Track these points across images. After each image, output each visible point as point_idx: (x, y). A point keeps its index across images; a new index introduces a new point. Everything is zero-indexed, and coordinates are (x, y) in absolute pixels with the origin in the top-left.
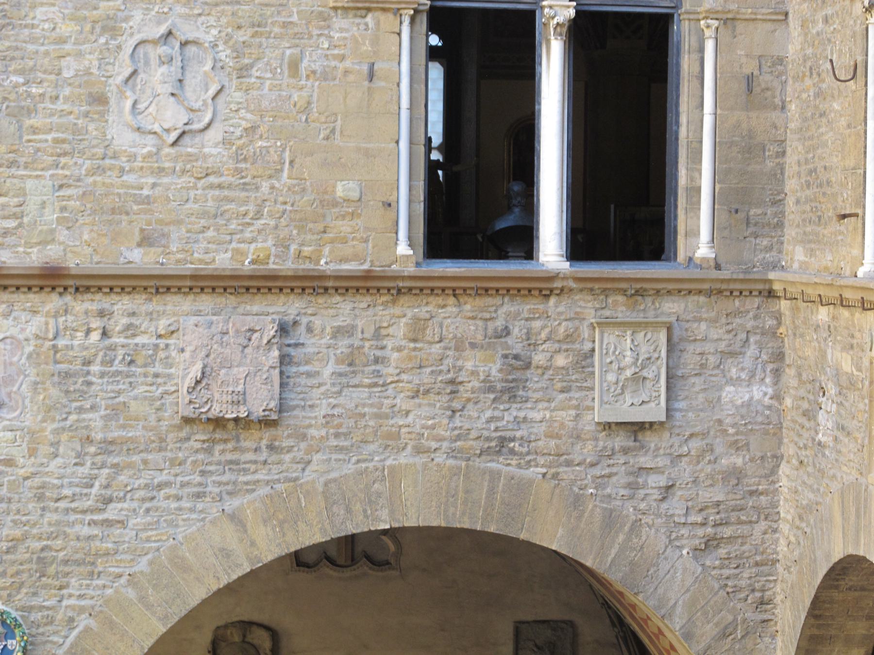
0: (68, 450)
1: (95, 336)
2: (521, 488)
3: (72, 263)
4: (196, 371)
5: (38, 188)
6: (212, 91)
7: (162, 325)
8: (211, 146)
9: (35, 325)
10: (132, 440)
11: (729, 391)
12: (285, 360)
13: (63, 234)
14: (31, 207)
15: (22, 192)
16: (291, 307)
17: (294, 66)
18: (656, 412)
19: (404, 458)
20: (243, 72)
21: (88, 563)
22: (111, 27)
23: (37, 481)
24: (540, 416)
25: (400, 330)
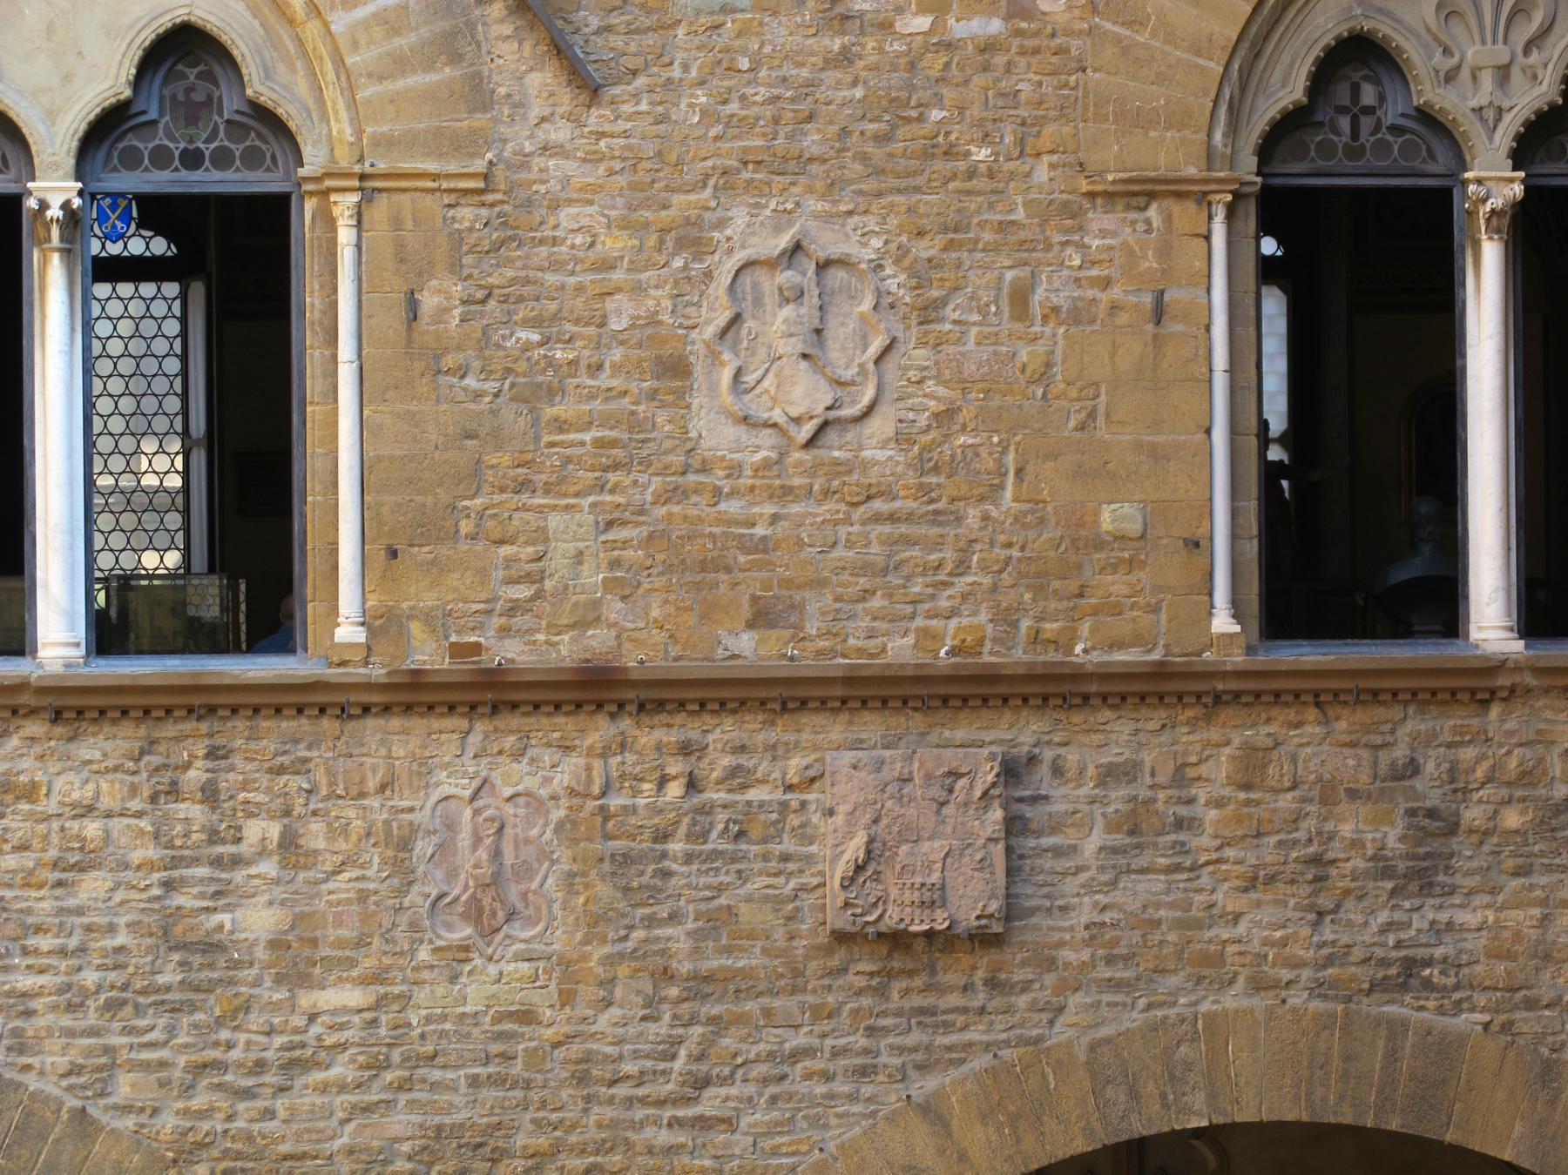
1: (675, 790)
2: (1445, 1050)
3: (631, 659)
4: (855, 848)
5: (569, 529)
6: (874, 349)
7: (794, 766)
8: (875, 445)
9: (567, 772)
10: (745, 973)
12: (1014, 826)
13: (614, 609)
14: (559, 561)
15: (541, 536)
16: (1025, 731)
17: (1020, 299)
19: (1233, 1000)
20: (928, 312)
22: (693, 239)
23: (576, 1049)
25: (1219, 769)
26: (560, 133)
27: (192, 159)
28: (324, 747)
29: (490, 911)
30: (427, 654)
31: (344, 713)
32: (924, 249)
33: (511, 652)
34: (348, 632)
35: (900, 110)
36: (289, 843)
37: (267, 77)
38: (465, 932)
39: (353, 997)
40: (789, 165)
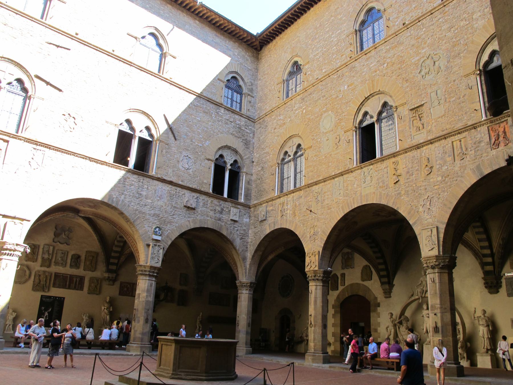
0: (170, 206)
2: (221, 226)
4: (187, 200)
5: (170, 171)
7: (183, 193)
11: (244, 219)
18: (237, 219)
19: (209, 218)
20: (195, 163)
21: (170, 223)
22: (181, 153)
24: (225, 217)
25: (210, 201)
29: (161, 197)
30: (159, 176)
31: (153, 179)
36: (147, 188)
39: (151, 201)
40: (188, 150)
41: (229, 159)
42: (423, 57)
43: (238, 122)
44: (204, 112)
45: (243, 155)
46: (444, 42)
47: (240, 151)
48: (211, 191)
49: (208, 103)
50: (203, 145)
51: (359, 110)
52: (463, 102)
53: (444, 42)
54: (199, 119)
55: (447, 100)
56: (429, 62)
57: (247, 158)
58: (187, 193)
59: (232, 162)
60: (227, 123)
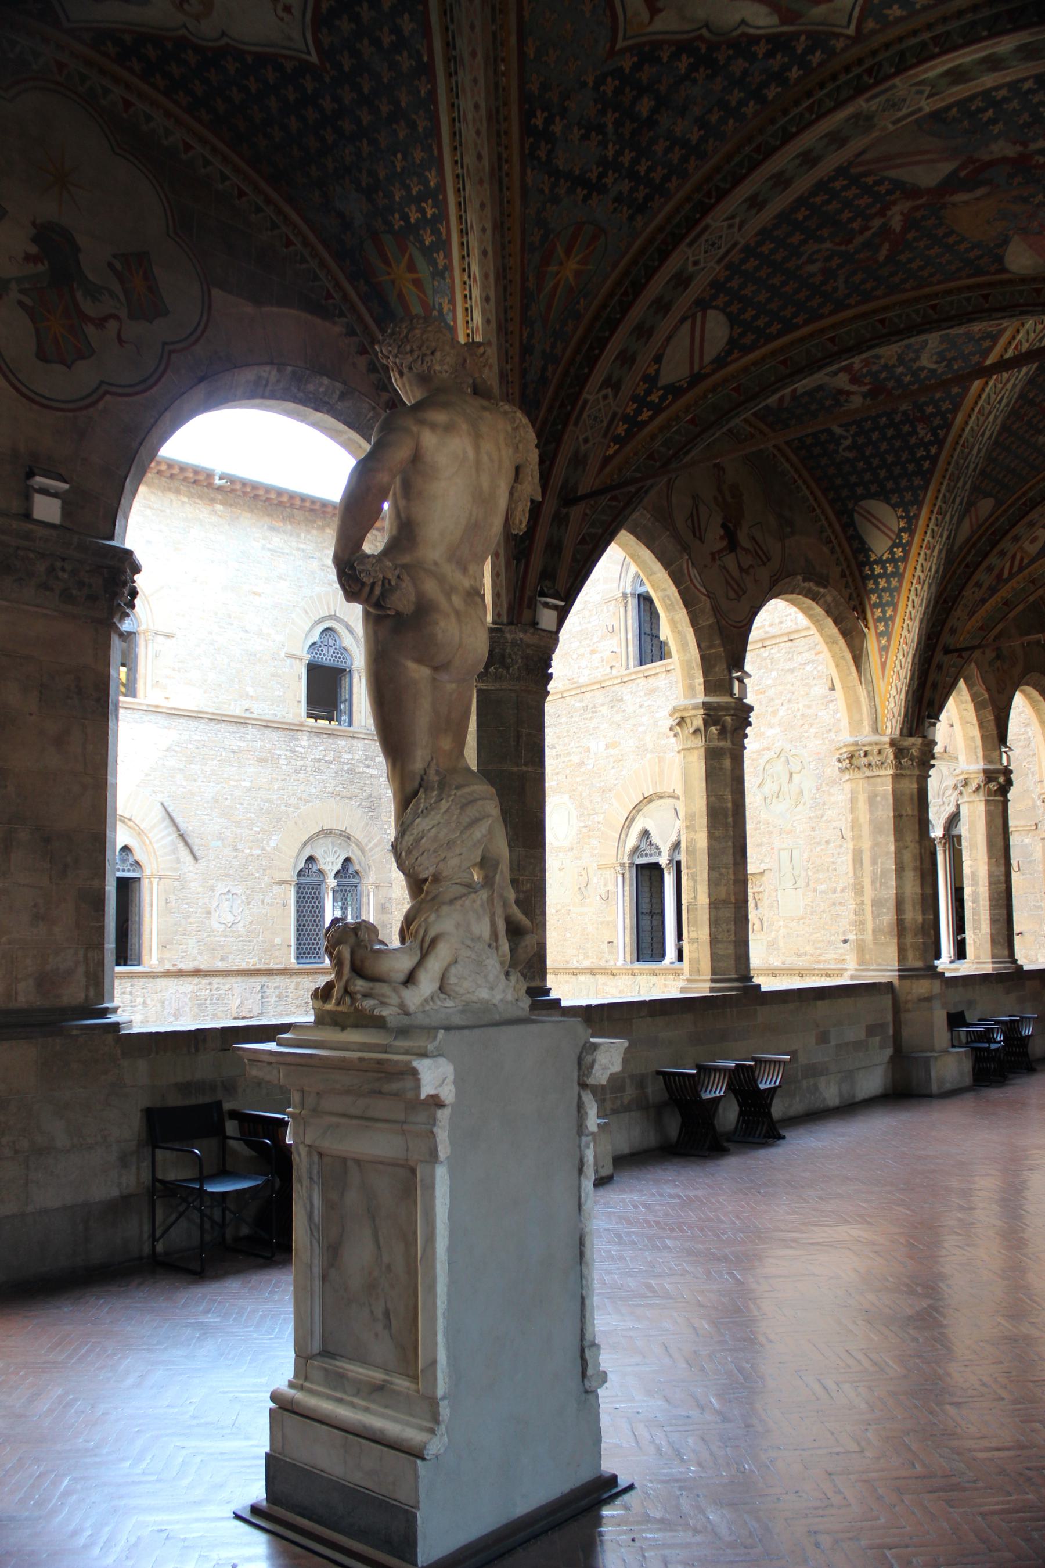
3: (202, 967)
4: (238, 1002)
5: (192, 942)
7: (227, 987)
8: (240, 927)
9: (190, 988)
12: (262, 997)
13: (199, 958)
15: (187, 944)
16: (263, 979)
17: (263, 902)
20: (249, 904)
22: (212, 889)
25: (292, 986)
26: (191, 869)
27: (124, 870)
28: (151, 983)
30: (168, 966)
31: (154, 977)
32: (248, 892)
33: (182, 966)
34: (154, 961)
35: (245, 866)
36: (144, 1002)
37: (139, 855)
38: (173, 1019)
40: (227, 876)
41: (330, 863)
42: (769, 749)
43: (346, 756)
44: (261, 760)
45: (364, 841)
46: (813, 730)
47: (357, 834)
48: (293, 960)
49: (267, 731)
50: (263, 849)
51: (630, 820)
52: (840, 903)
53: (813, 730)
54: (248, 784)
55: (812, 885)
56: (779, 767)
57: (376, 845)
58: (237, 984)
59: (339, 867)
60: (318, 770)
